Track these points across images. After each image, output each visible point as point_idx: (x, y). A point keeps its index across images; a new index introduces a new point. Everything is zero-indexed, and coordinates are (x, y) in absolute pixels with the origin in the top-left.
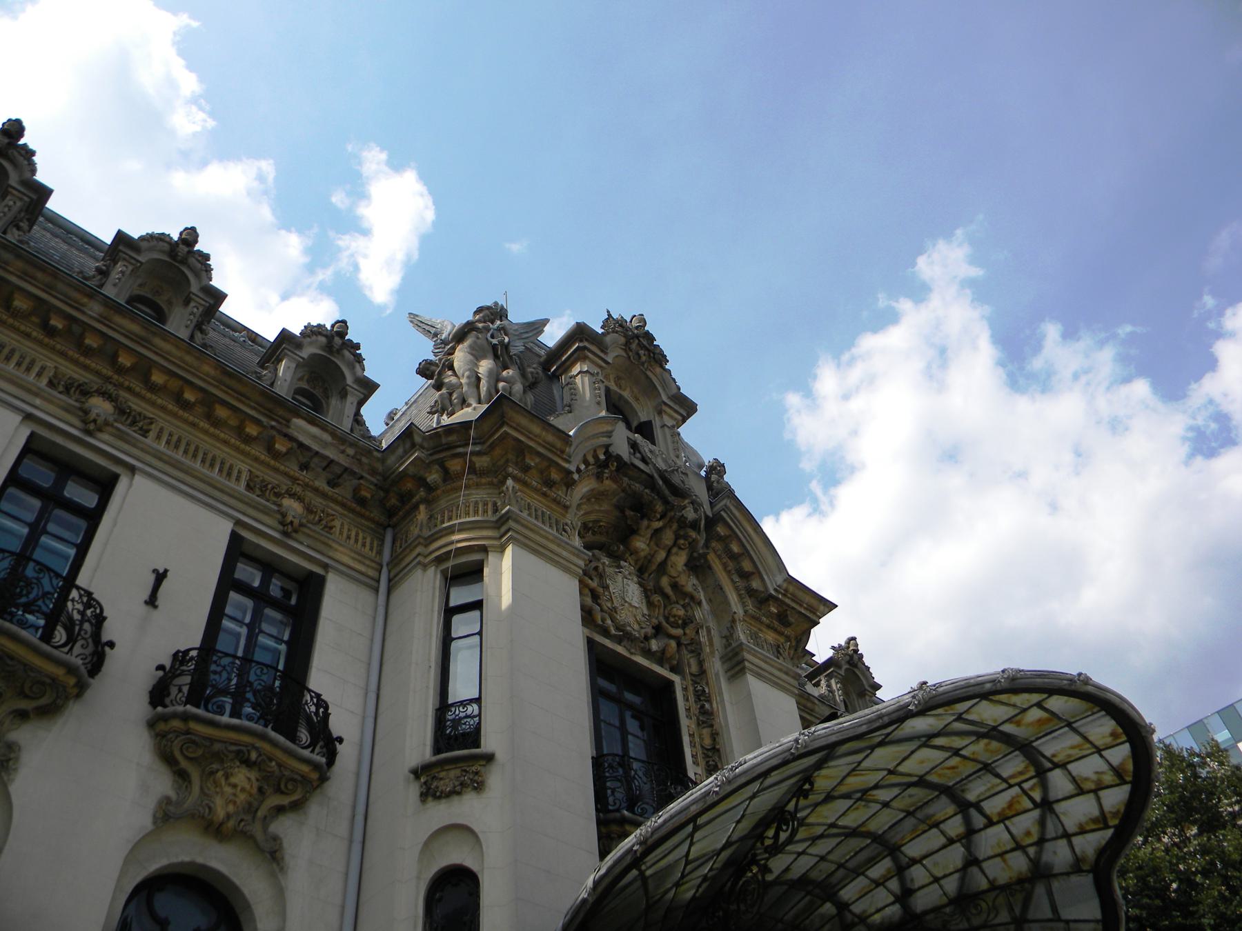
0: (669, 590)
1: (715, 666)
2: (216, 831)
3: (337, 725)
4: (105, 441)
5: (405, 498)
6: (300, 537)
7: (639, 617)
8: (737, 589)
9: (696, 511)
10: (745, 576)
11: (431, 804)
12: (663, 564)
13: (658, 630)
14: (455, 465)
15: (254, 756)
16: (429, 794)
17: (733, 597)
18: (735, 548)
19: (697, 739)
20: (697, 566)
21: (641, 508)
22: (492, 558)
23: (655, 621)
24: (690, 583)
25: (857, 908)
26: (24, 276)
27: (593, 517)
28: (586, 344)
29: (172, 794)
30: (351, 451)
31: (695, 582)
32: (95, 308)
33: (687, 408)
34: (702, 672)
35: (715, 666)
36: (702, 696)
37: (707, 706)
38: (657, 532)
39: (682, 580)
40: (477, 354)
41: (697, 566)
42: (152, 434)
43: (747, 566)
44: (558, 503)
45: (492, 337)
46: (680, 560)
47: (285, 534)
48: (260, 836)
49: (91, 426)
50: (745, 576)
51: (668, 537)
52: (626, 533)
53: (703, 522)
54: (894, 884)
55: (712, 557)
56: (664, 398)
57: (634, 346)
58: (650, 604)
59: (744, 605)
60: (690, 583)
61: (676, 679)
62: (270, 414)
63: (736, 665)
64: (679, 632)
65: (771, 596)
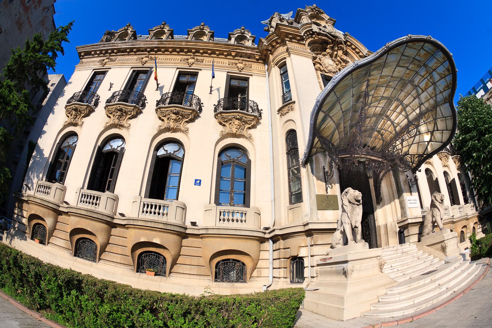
0: (340, 60)
4: (194, 67)
11: (283, 117)
12: (336, 55)
15: (238, 117)
18: (353, 47)
20: (346, 53)
21: (327, 43)
24: (345, 57)
29: (223, 130)
41: (346, 53)
44: (302, 44)
46: (340, 53)
48: (246, 135)
54: (403, 113)
55: (348, 50)
58: (337, 65)
60: (345, 57)
62: (228, 48)
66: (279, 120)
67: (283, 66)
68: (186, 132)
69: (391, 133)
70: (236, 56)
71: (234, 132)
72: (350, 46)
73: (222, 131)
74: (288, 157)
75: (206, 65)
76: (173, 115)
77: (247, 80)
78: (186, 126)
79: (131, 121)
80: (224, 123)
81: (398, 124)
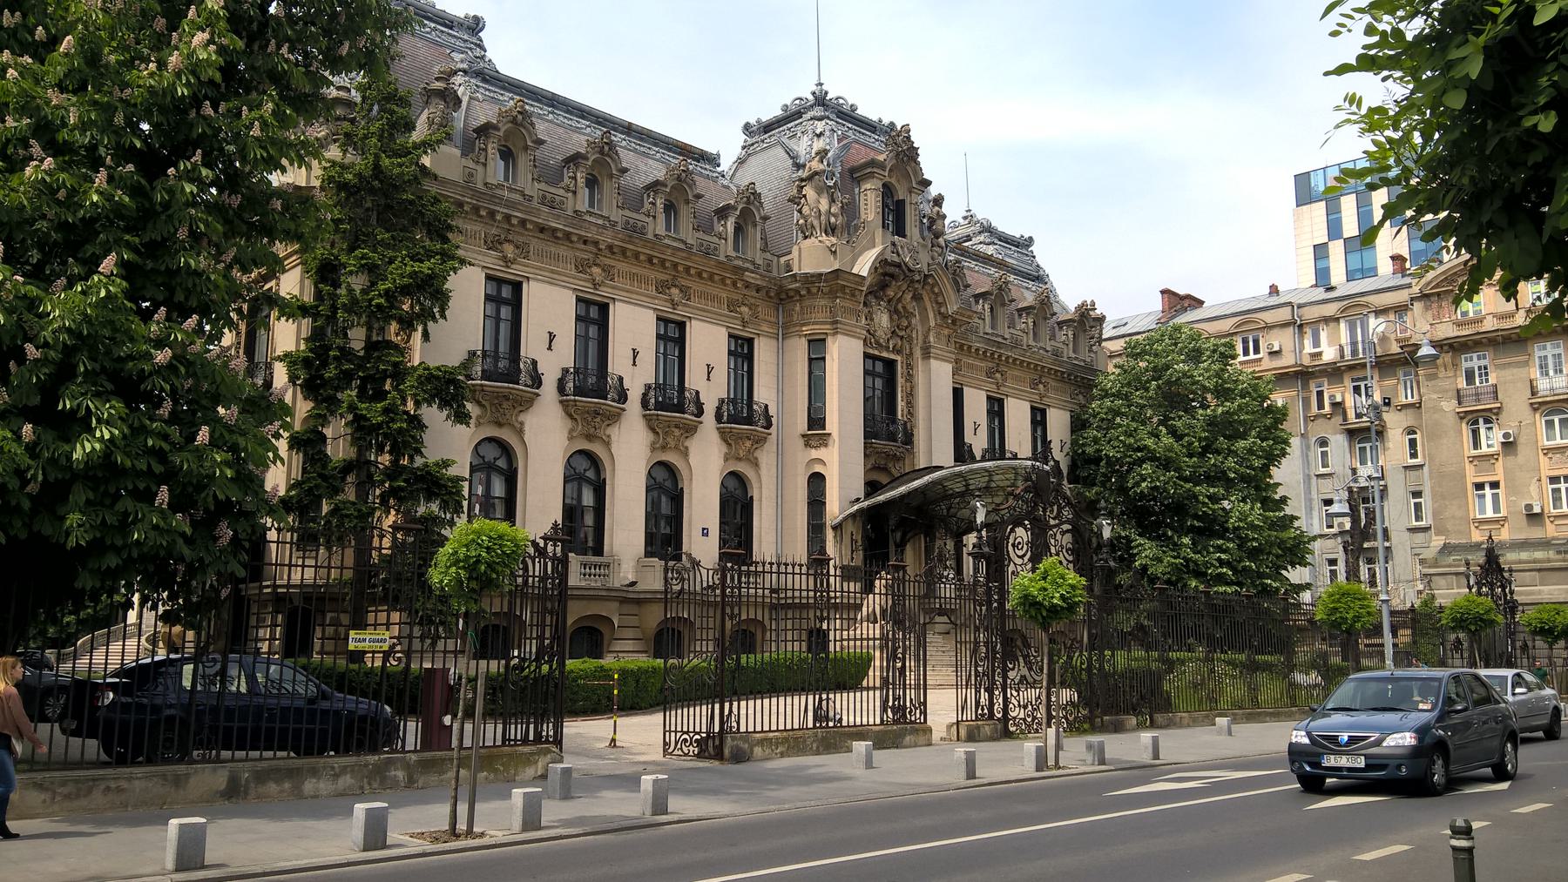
1: (918, 353)
2: (740, 459)
3: (772, 411)
10: (940, 304)
14: (814, 290)
16: (807, 445)
17: (931, 315)
24: (912, 306)
26: (644, 247)
32: (669, 251)
33: (928, 183)
35: (918, 353)
36: (909, 366)
40: (819, 191)
41: (917, 298)
43: (940, 299)
46: (908, 296)
49: (674, 305)
52: (883, 286)
60: (912, 306)
61: (899, 358)
63: (927, 355)
67: (817, 346)
68: (685, 453)
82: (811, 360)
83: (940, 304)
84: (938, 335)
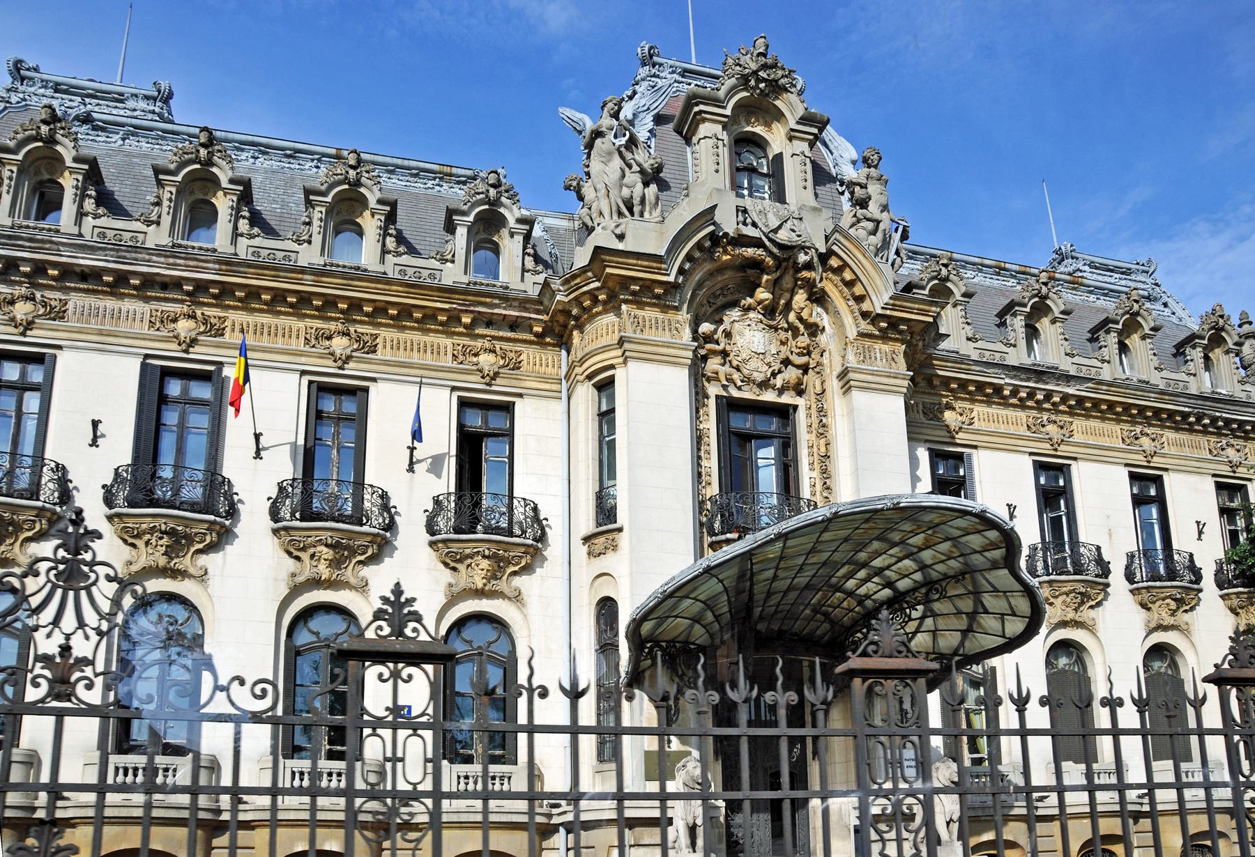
1: (834, 385)
2: (480, 593)
5: (565, 326)
6: (498, 381)
7: (769, 359)
8: (852, 312)
9: (806, 254)
11: (593, 559)
13: (786, 362)
17: (848, 320)
19: (815, 449)
20: (818, 298)
22: (619, 374)
23: (782, 356)
25: (862, 591)
27: (718, 286)
28: (702, 107)
30: (516, 304)
31: (820, 310)
34: (824, 391)
37: (824, 420)
38: (776, 282)
39: (805, 315)
41: (818, 298)
42: (380, 347)
43: (858, 290)
45: (616, 137)
46: (800, 298)
47: (487, 384)
50: (859, 299)
51: (787, 282)
53: (816, 259)
56: (793, 125)
57: (753, 83)
59: (857, 325)
64: (804, 360)
65: (878, 315)
66: (585, 568)
69: (851, 611)
70: (474, 323)
71: (480, 585)
72: (838, 271)
73: (450, 585)
74: (598, 659)
75: (386, 363)
76: (325, 550)
77: (508, 408)
78: (362, 574)
79: (203, 560)
80: (452, 564)
81: (868, 597)
82: (602, 415)
83: (859, 299)
84: (865, 356)
